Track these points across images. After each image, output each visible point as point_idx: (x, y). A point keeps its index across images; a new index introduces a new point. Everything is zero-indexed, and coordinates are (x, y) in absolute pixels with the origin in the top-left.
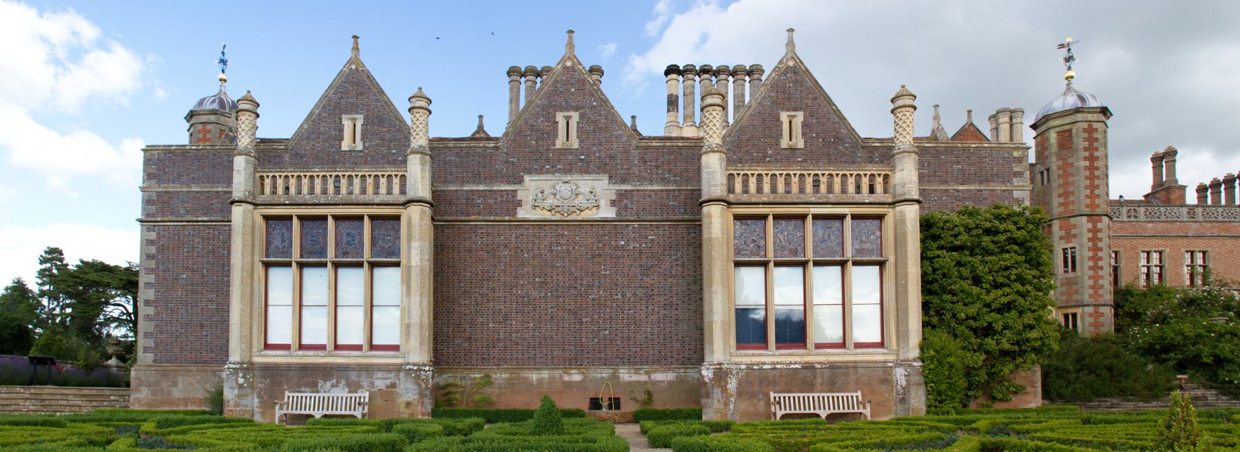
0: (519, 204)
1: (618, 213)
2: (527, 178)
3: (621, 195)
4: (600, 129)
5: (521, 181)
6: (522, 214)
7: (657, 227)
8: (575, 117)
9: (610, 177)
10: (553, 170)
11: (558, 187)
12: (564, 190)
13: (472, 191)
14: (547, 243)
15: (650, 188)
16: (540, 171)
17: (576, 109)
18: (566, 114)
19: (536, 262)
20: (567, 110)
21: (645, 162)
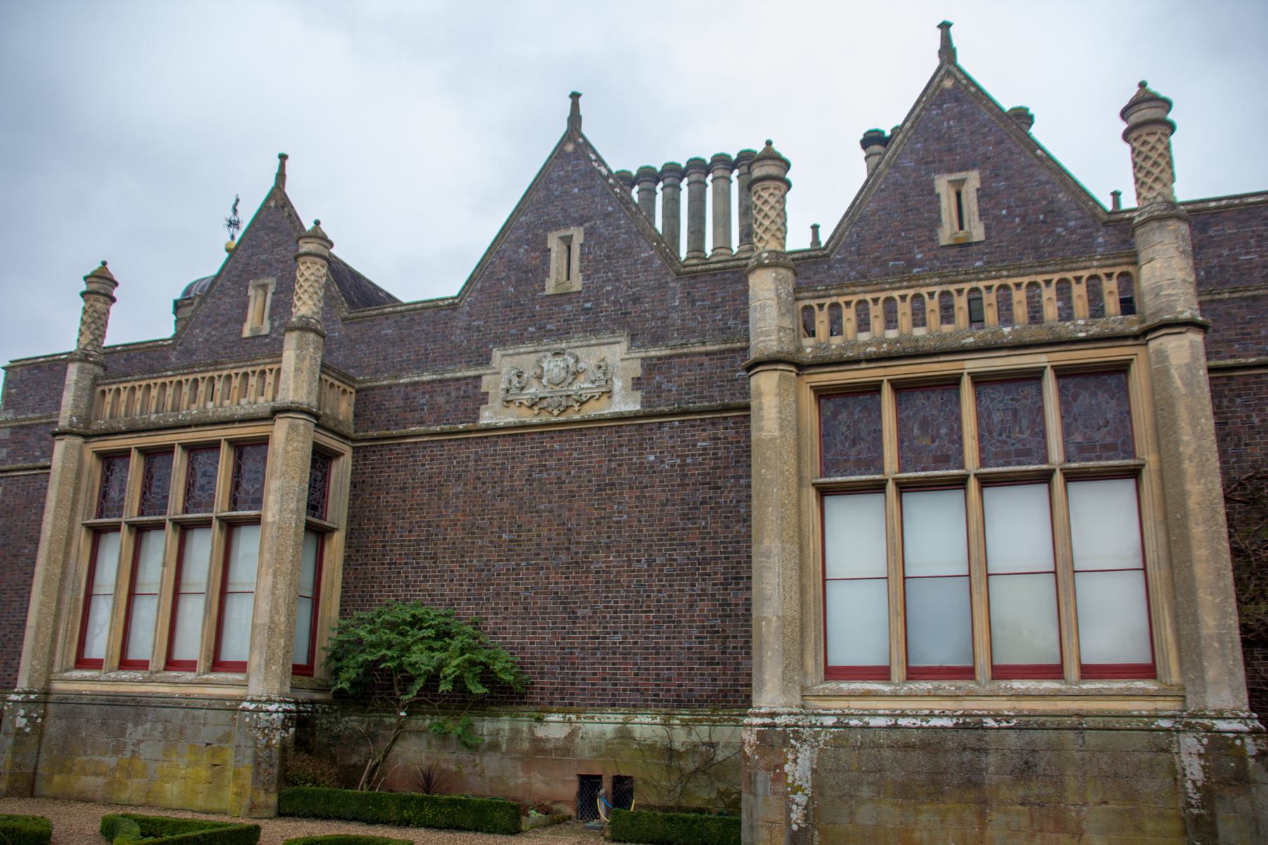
0: (484, 399)
1: (646, 401)
2: (497, 353)
3: (651, 366)
4: (619, 251)
5: (486, 360)
6: (487, 417)
7: (714, 423)
8: (578, 235)
9: (633, 338)
10: (544, 334)
11: (545, 365)
12: (554, 367)
13: (415, 384)
14: (524, 467)
15: (700, 349)
16: (519, 339)
17: (580, 222)
18: (563, 233)
19: (505, 505)
20: (567, 226)
21: (693, 301)
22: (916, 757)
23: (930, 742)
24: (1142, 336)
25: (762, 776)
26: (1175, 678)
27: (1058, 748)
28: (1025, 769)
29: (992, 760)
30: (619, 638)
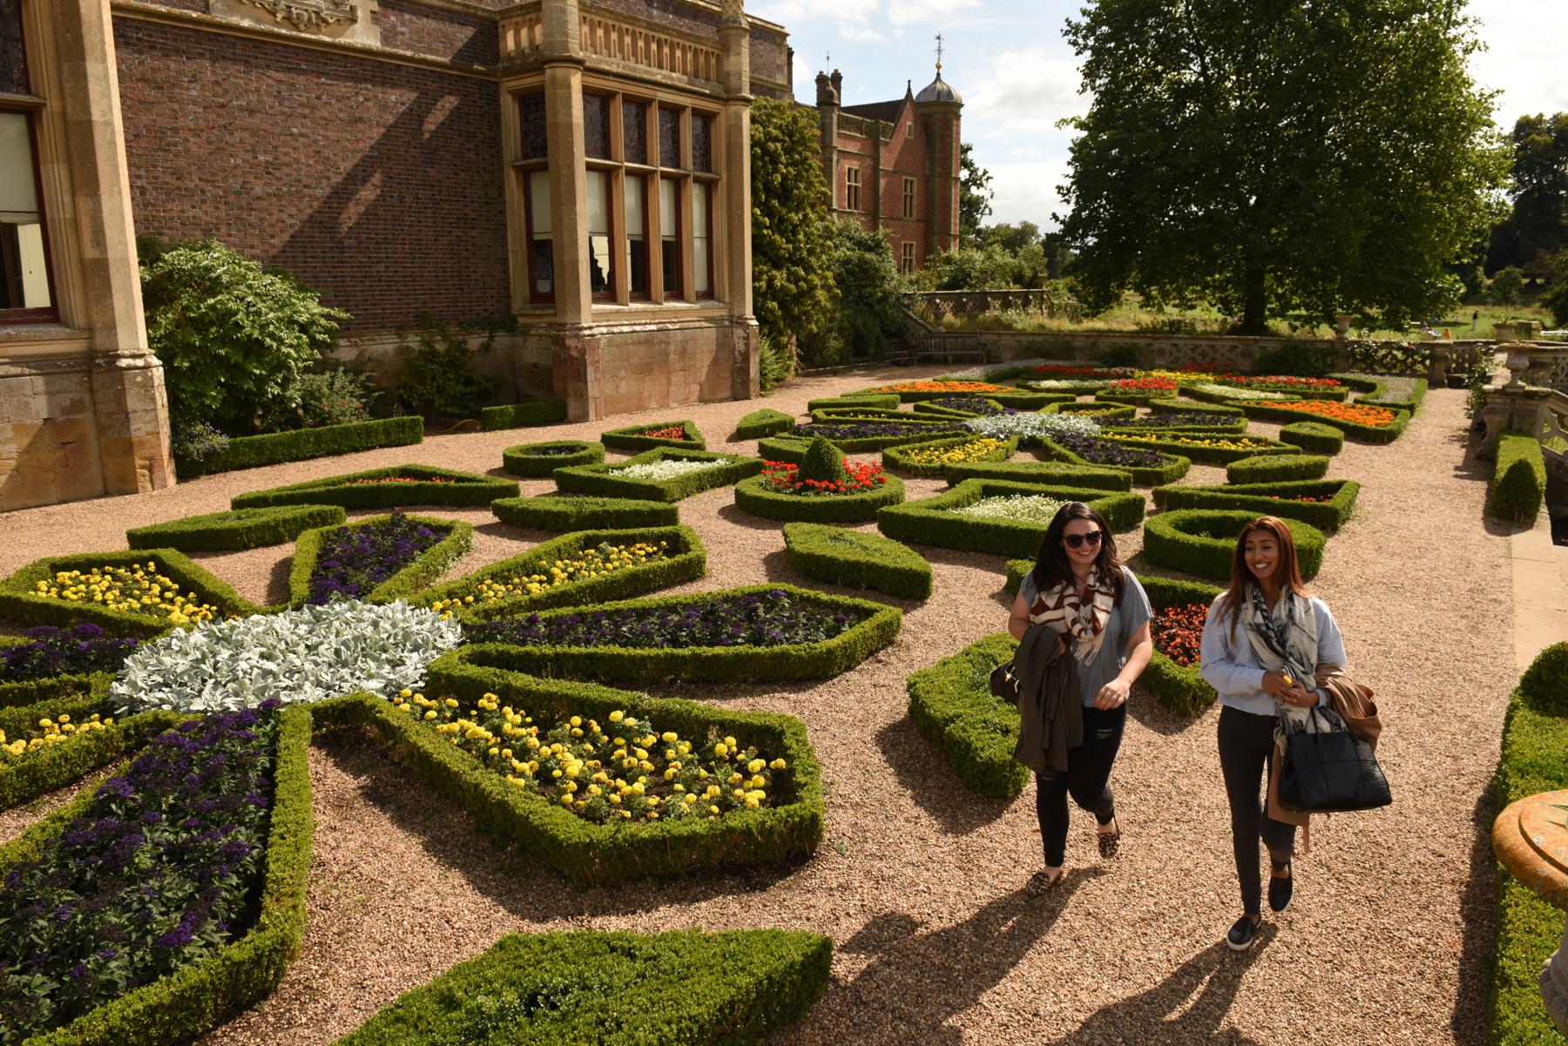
1: (385, 39)
22: (642, 350)
23: (647, 340)
24: (726, 101)
25: (590, 370)
26: (727, 299)
27: (694, 339)
28: (683, 353)
29: (672, 347)
30: (381, 267)
